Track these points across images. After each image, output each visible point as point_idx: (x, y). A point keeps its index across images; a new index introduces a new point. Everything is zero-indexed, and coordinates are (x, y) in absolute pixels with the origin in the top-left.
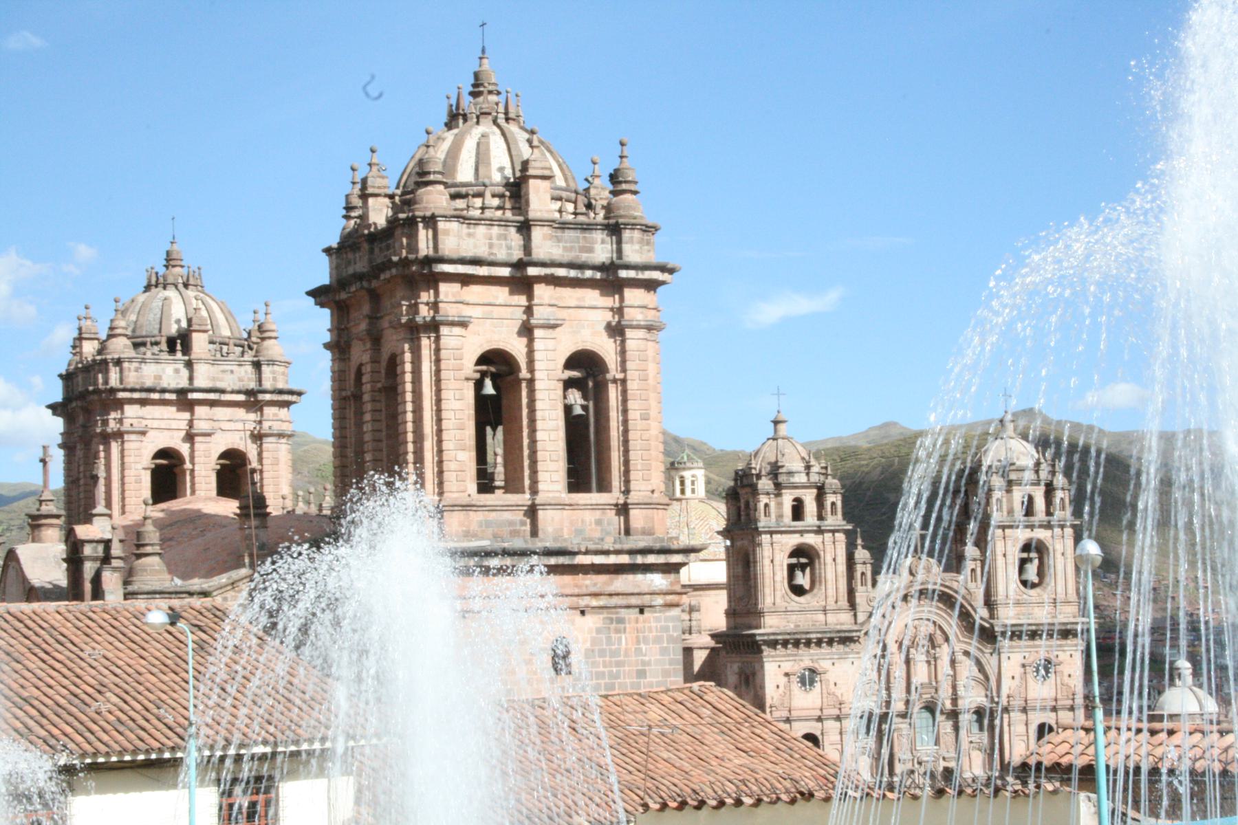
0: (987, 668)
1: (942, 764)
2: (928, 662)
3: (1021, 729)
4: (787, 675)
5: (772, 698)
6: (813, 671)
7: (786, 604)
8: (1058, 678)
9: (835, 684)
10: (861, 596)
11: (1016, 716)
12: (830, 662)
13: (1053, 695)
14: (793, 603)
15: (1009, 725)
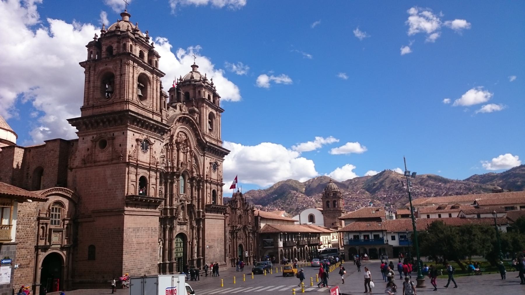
0: (199, 161)
1: (187, 203)
2: (183, 153)
3: (209, 190)
4: (137, 140)
5: (130, 152)
6: (147, 141)
9: (155, 152)
10: (164, 112)
11: (208, 185)
12: (154, 140)
15: (206, 189)
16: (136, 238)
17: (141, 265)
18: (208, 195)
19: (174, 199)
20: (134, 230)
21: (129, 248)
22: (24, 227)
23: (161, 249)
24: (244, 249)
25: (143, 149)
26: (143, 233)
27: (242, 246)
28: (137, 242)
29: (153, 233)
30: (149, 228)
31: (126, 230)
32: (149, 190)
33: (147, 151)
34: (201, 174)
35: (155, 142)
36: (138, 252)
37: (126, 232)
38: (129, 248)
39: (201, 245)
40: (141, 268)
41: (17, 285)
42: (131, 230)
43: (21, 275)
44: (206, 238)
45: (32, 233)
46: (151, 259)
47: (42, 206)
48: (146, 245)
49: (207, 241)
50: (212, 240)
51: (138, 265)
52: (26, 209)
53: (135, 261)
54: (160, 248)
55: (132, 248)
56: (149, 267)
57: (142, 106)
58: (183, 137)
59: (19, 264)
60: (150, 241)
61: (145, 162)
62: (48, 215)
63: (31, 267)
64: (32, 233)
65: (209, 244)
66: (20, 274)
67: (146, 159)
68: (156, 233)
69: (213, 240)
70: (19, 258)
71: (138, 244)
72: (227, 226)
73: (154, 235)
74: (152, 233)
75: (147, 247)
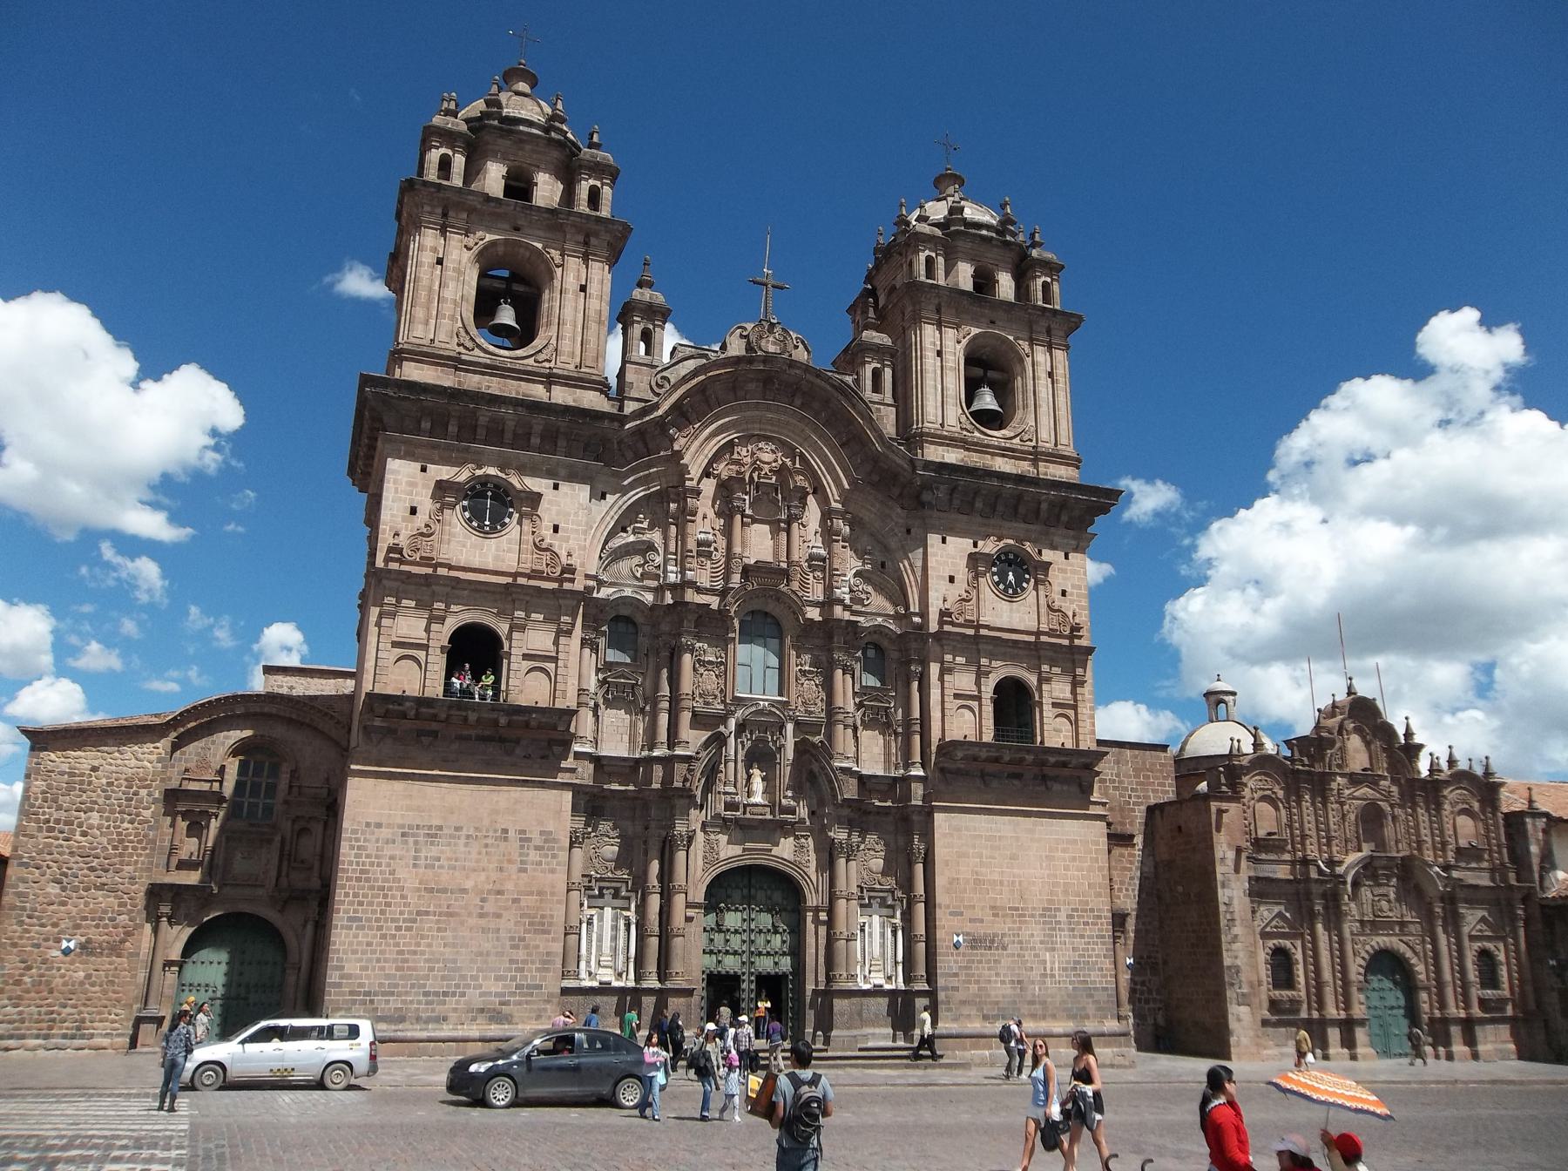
3: (963, 681)
4: (442, 488)
5: (396, 534)
7: (461, 349)
8: (1042, 593)
9: (556, 529)
12: (551, 482)
13: (1031, 624)
14: (477, 352)
16: (415, 866)
17: (443, 978)
18: (952, 704)
19: (686, 717)
20: (403, 835)
21: (371, 904)
22: (108, 820)
23: (633, 928)
24: (1422, 977)
25: (476, 514)
26: (462, 849)
27: (1407, 960)
28: (420, 884)
29: (533, 856)
30: (505, 831)
31: (354, 832)
32: (508, 678)
33: (504, 525)
34: (915, 608)
35: (556, 487)
36: (429, 923)
37: (357, 840)
38: (371, 904)
39: (920, 929)
40: (445, 994)
41: (68, 1010)
42: (385, 833)
43: (88, 976)
44: (941, 897)
45: (139, 842)
46: (511, 961)
47: (198, 754)
48: (483, 900)
49: (951, 913)
50: (993, 908)
51: (427, 977)
52: (119, 762)
53: (406, 961)
54: (628, 926)
55: (388, 905)
56: (503, 995)
57: (488, 362)
58: (767, 457)
59: (83, 939)
60: (509, 886)
61: (491, 567)
62: (216, 785)
63: (131, 955)
64: (139, 842)
65: (969, 927)
66: (82, 974)
67: (496, 558)
68: (554, 856)
69: (1019, 914)
70: (85, 918)
71: (431, 890)
72: (1231, 855)
73: (540, 863)
74: (521, 854)
75: (490, 907)
